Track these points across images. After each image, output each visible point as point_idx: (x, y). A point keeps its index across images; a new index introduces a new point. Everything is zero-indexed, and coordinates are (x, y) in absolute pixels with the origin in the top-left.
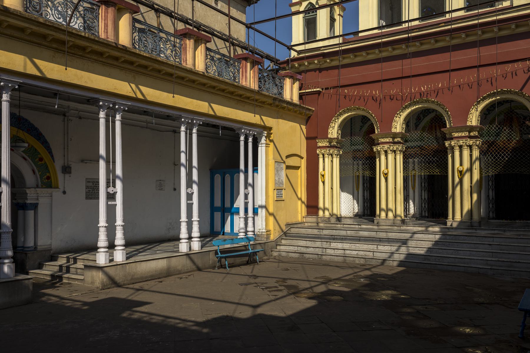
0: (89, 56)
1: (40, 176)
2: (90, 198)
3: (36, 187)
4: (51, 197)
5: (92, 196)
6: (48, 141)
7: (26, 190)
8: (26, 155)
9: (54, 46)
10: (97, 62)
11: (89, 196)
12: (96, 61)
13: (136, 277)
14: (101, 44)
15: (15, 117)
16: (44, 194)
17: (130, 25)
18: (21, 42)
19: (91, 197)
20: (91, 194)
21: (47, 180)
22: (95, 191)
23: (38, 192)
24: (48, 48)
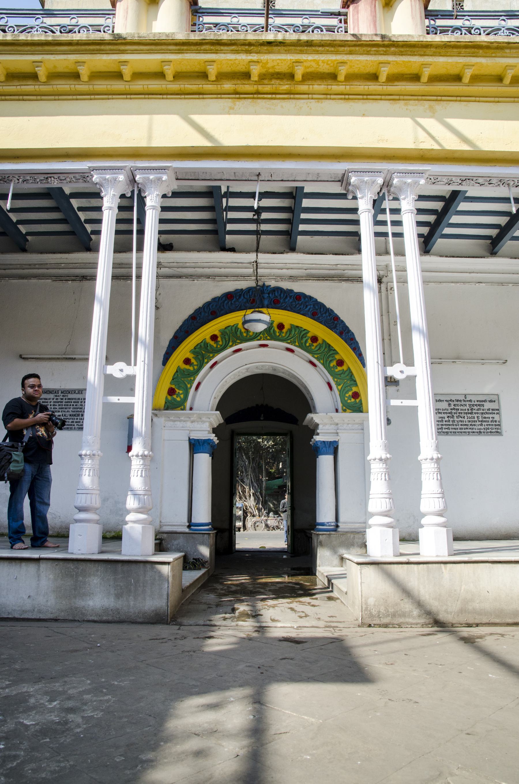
0: (304, 88)
1: (340, 391)
2: (444, 432)
3: (335, 410)
4: (361, 431)
5: (448, 429)
6: (350, 329)
7: (312, 418)
8: (313, 356)
9: (228, 86)
10: (329, 96)
11: (442, 428)
12: (327, 95)
13: (477, 605)
14: (320, 49)
15: (291, 295)
16: (348, 424)
17: (413, 18)
18: (167, 98)
19: (446, 430)
20: (445, 425)
21: (353, 400)
22: (455, 419)
23: (336, 421)
24: (219, 96)
